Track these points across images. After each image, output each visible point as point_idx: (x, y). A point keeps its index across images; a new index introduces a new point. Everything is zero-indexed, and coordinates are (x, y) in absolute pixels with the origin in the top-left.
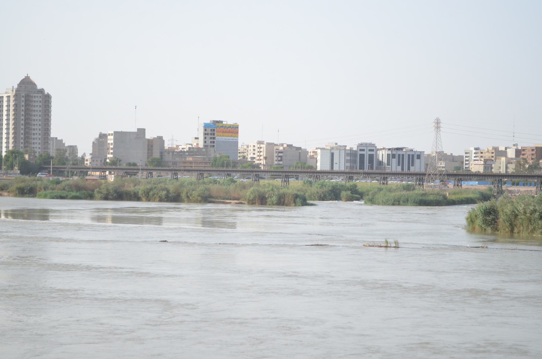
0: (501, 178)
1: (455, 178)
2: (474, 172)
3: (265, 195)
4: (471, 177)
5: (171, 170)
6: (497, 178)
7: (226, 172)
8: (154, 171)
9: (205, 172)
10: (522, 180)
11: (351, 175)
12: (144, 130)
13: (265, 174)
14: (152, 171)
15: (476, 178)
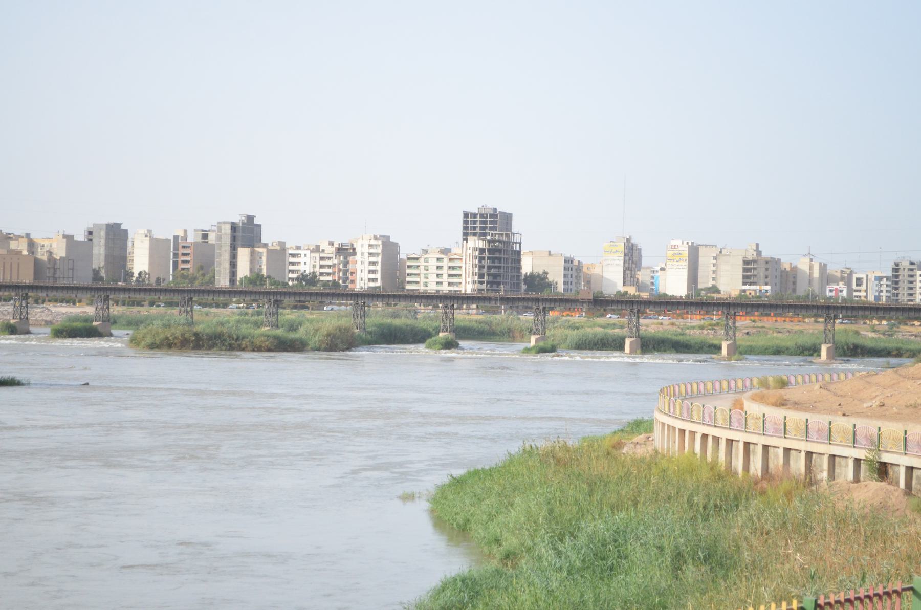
0: (26, 292)
1: (631, 307)
2: (613, 296)
3: (560, 348)
4: (324, 299)
5: (268, 293)
6: (102, 293)
7: (272, 297)
8: (31, 291)
9: (287, 297)
10: (149, 297)
11: (278, 298)
12: (511, 215)
13: (93, 293)
14: (282, 298)
15: (86, 296)
